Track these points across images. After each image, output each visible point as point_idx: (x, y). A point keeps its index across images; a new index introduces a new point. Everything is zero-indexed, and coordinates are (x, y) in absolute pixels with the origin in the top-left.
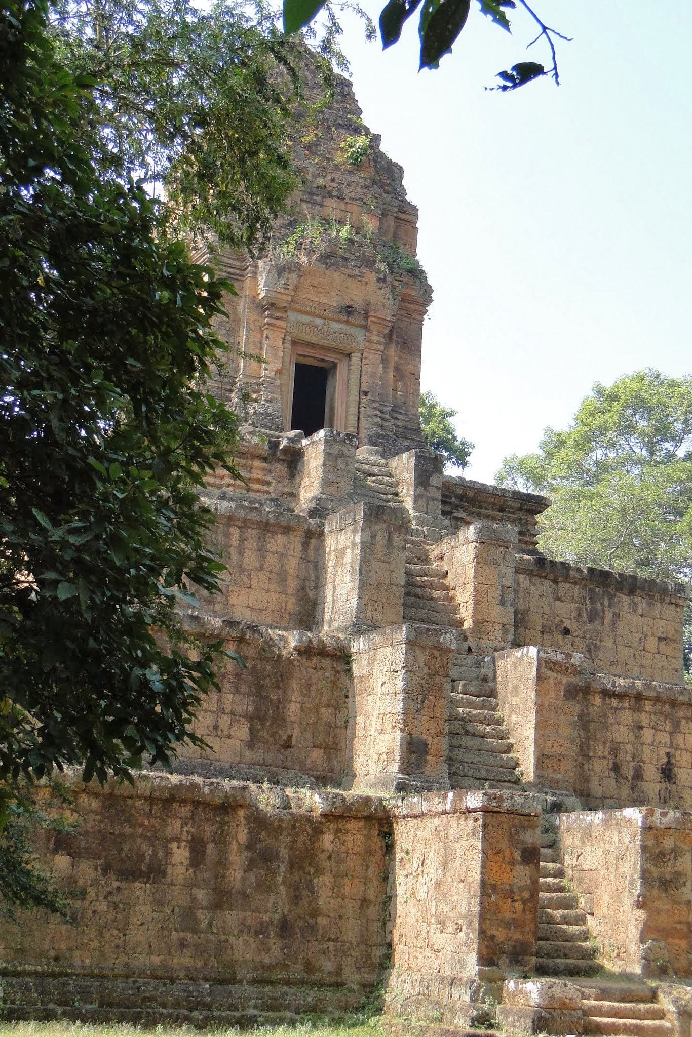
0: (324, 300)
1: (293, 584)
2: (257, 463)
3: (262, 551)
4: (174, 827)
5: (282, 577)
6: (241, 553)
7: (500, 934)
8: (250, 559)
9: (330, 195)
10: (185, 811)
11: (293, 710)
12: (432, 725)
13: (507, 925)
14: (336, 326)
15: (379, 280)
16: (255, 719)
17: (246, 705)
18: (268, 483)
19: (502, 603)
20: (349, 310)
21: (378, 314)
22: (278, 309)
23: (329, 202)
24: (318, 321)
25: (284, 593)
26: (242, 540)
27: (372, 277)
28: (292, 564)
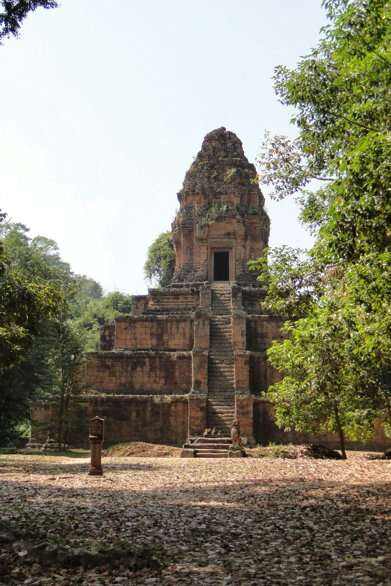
0: (219, 233)
1: (187, 336)
2: (189, 296)
3: (178, 328)
4: (132, 407)
5: (184, 334)
6: (171, 330)
7: (195, 428)
8: (174, 330)
9: (222, 194)
10: (134, 404)
11: (177, 373)
12: (202, 376)
13: (197, 426)
14: (225, 240)
15: (237, 222)
16: (166, 378)
17: (163, 374)
18: (193, 302)
19: (242, 335)
20: (228, 234)
21: (239, 233)
22: (204, 240)
23: (222, 196)
24: (219, 240)
25: (185, 339)
26: (171, 326)
27: (235, 221)
28: (187, 331)
